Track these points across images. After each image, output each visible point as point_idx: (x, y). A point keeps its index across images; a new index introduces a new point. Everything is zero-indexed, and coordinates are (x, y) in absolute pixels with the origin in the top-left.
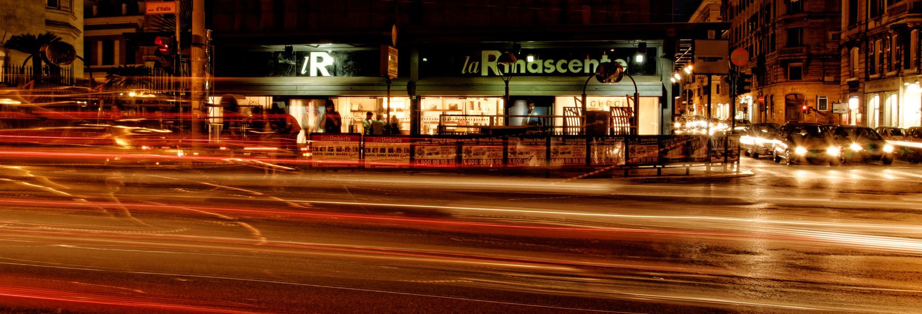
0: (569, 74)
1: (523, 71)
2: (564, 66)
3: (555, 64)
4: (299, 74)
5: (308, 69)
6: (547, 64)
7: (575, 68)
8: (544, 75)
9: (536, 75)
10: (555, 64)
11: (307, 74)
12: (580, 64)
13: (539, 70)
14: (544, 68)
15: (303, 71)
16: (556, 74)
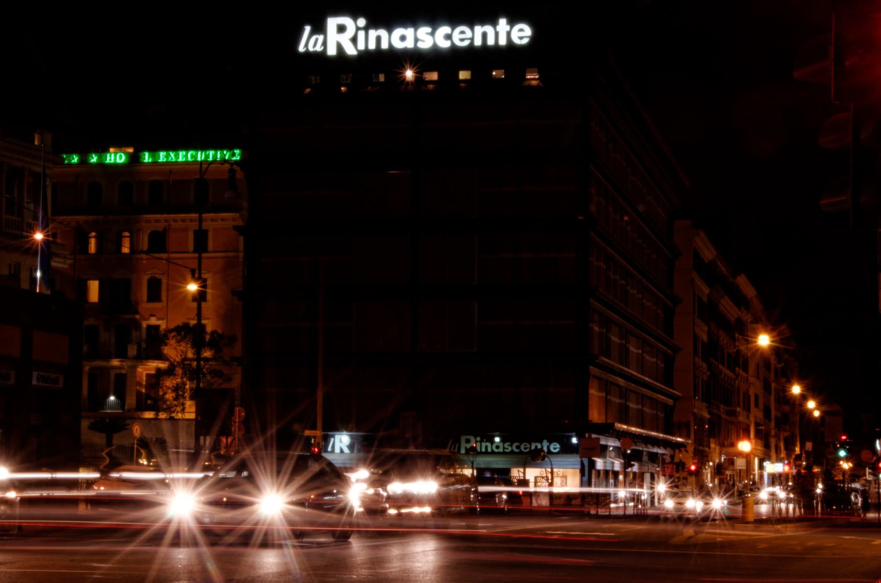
0: (521, 453)
1: (489, 450)
2: (518, 447)
3: (511, 446)
4: (326, 451)
5: (333, 447)
6: (506, 445)
7: (525, 449)
8: (504, 453)
9: (499, 453)
10: (511, 446)
11: (333, 451)
12: (528, 446)
13: (501, 450)
14: (504, 448)
15: (329, 449)
16: (512, 452)
